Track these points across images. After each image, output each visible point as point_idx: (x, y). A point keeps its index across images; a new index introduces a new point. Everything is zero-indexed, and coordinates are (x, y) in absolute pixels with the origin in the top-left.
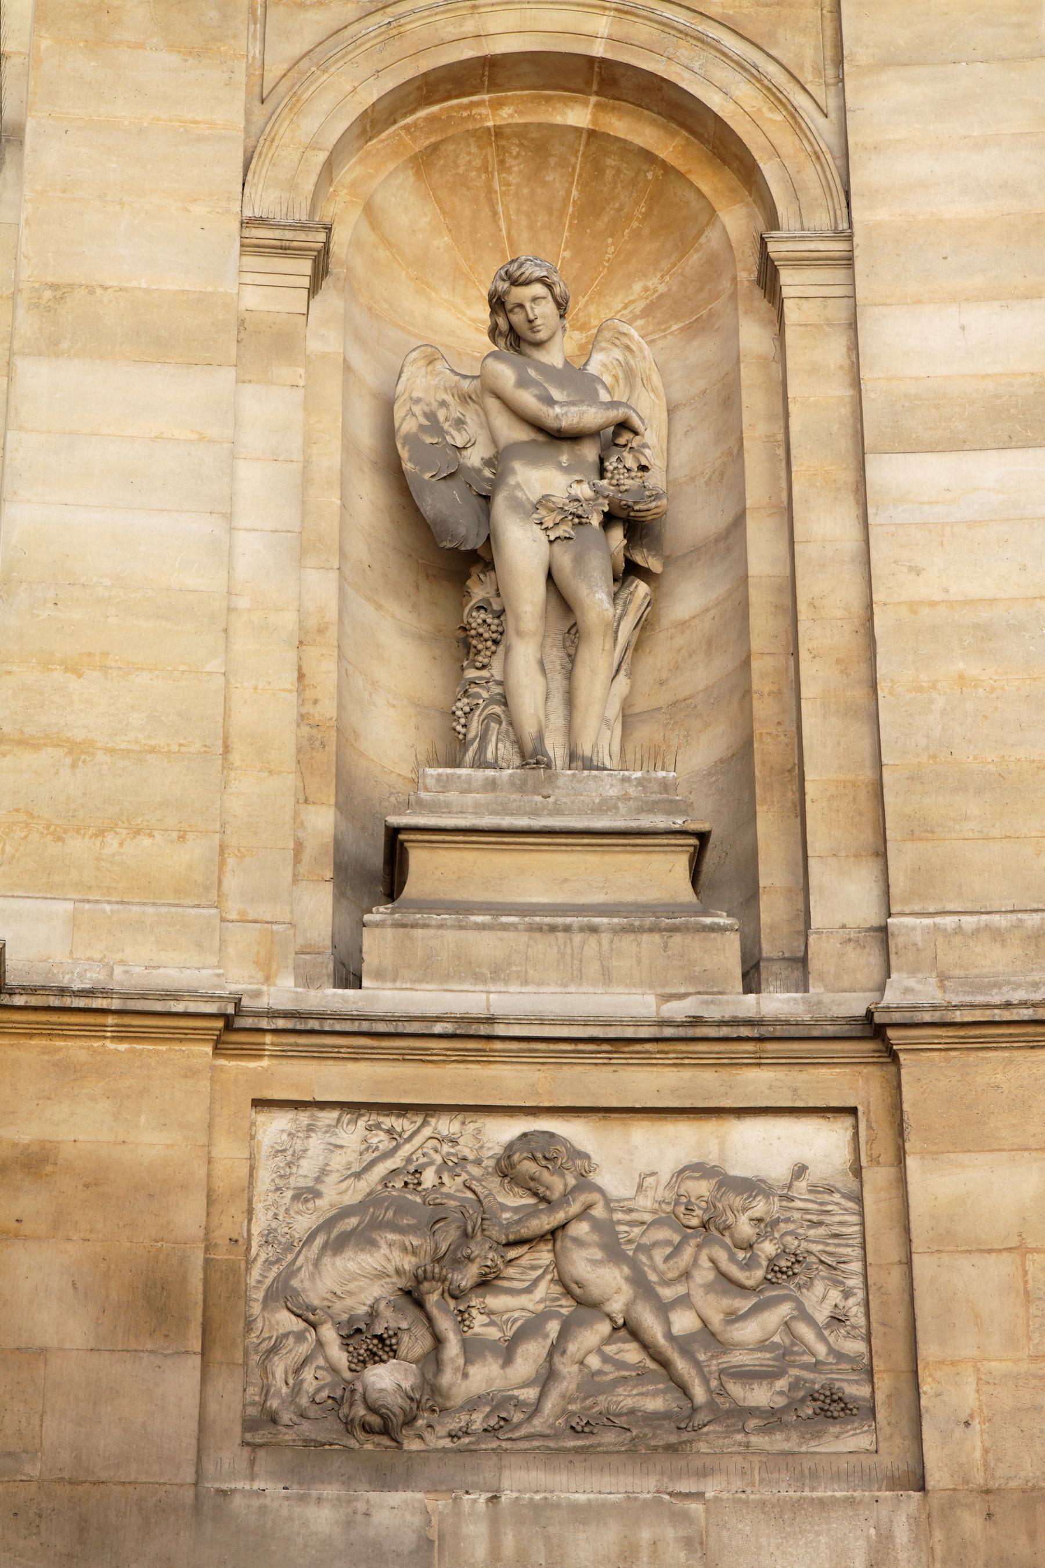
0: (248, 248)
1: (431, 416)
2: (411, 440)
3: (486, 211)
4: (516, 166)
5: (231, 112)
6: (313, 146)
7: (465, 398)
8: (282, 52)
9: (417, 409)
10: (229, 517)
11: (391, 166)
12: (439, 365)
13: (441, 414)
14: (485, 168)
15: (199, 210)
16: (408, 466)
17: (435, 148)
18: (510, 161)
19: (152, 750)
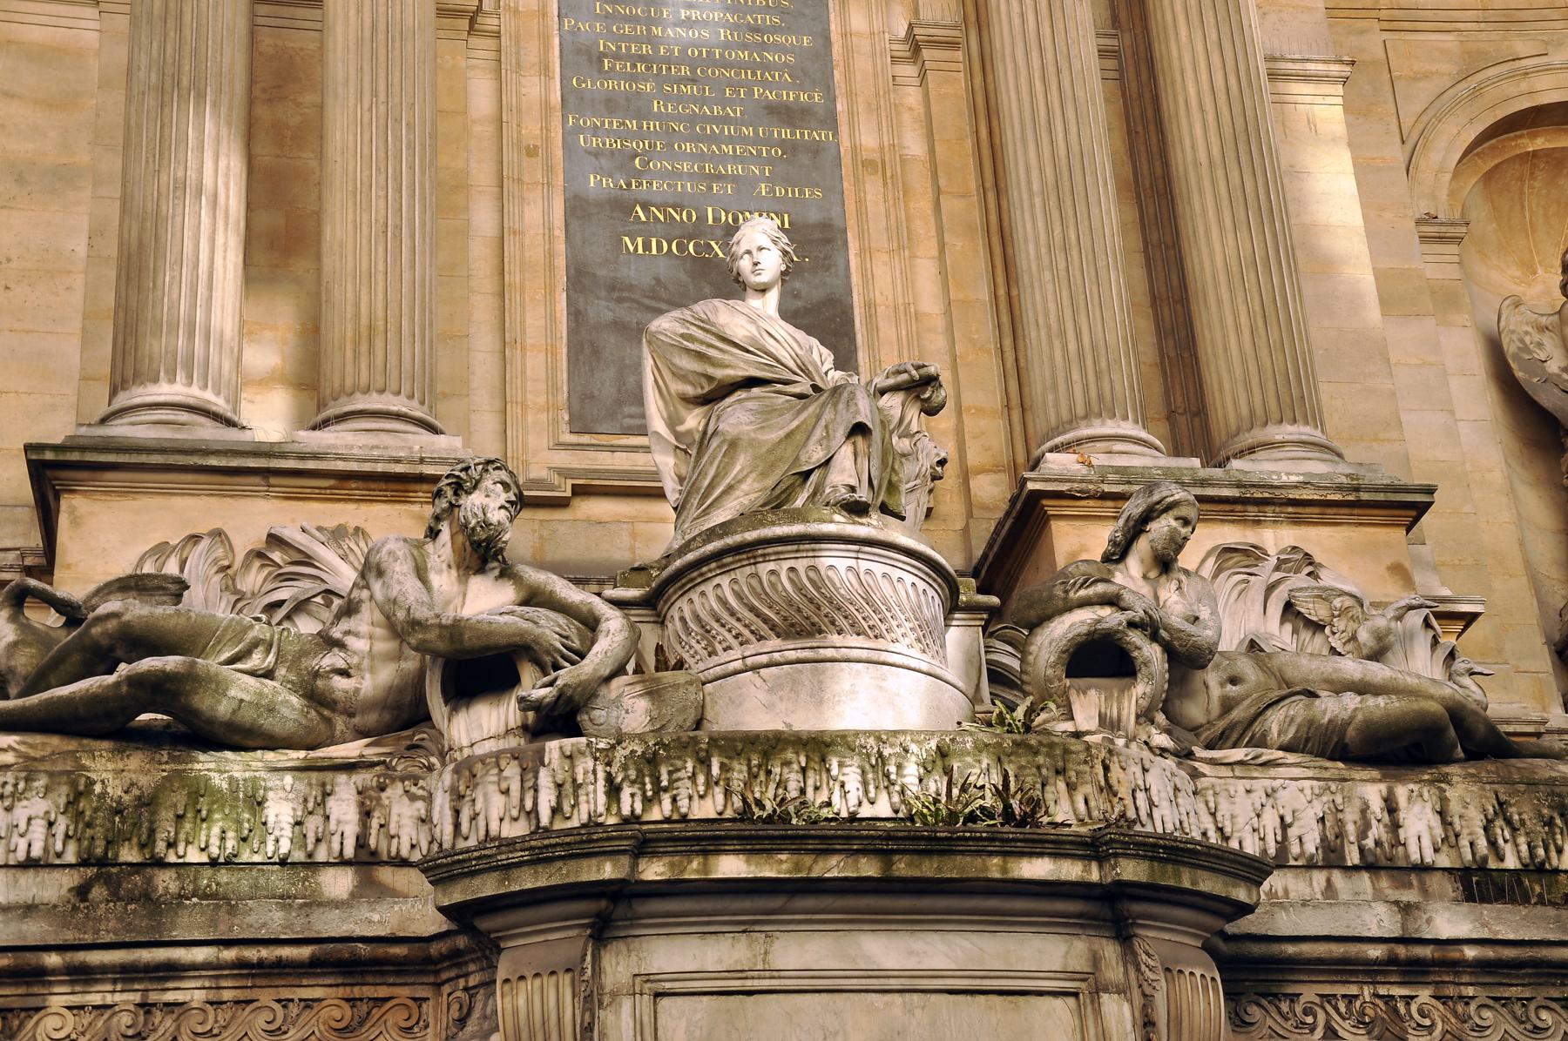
0: (1424, 239)
1: (1522, 341)
2: (1516, 357)
3: (1518, 207)
4: (1540, 175)
5: (1398, 154)
6: (1441, 170)
7: (1542, 329)
8: (1410, 110)
9: (1514, 337)
10: (1452, 412)
11: (1474, 180)
12: (1522, 308)
13: (1527, 339)
14: (1521, 179)
15: (1387, 215)
16: (1519, 374)
17: (1497, 166)
18: (1537, 173)
19: (1443, 564)
